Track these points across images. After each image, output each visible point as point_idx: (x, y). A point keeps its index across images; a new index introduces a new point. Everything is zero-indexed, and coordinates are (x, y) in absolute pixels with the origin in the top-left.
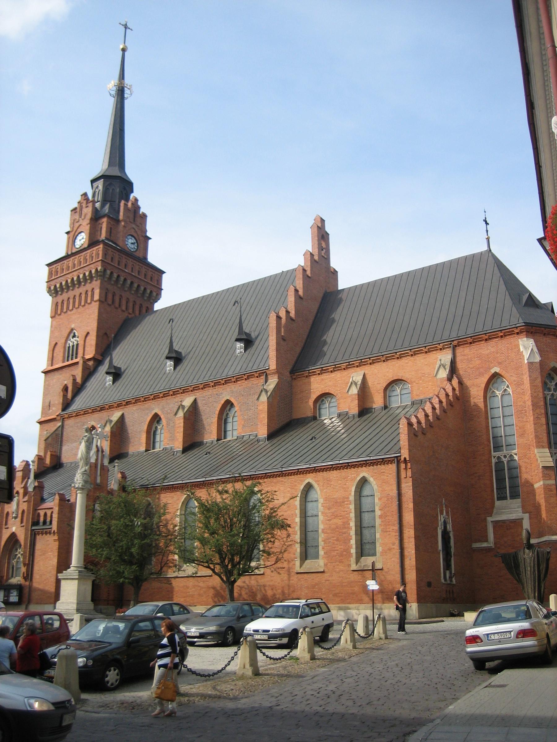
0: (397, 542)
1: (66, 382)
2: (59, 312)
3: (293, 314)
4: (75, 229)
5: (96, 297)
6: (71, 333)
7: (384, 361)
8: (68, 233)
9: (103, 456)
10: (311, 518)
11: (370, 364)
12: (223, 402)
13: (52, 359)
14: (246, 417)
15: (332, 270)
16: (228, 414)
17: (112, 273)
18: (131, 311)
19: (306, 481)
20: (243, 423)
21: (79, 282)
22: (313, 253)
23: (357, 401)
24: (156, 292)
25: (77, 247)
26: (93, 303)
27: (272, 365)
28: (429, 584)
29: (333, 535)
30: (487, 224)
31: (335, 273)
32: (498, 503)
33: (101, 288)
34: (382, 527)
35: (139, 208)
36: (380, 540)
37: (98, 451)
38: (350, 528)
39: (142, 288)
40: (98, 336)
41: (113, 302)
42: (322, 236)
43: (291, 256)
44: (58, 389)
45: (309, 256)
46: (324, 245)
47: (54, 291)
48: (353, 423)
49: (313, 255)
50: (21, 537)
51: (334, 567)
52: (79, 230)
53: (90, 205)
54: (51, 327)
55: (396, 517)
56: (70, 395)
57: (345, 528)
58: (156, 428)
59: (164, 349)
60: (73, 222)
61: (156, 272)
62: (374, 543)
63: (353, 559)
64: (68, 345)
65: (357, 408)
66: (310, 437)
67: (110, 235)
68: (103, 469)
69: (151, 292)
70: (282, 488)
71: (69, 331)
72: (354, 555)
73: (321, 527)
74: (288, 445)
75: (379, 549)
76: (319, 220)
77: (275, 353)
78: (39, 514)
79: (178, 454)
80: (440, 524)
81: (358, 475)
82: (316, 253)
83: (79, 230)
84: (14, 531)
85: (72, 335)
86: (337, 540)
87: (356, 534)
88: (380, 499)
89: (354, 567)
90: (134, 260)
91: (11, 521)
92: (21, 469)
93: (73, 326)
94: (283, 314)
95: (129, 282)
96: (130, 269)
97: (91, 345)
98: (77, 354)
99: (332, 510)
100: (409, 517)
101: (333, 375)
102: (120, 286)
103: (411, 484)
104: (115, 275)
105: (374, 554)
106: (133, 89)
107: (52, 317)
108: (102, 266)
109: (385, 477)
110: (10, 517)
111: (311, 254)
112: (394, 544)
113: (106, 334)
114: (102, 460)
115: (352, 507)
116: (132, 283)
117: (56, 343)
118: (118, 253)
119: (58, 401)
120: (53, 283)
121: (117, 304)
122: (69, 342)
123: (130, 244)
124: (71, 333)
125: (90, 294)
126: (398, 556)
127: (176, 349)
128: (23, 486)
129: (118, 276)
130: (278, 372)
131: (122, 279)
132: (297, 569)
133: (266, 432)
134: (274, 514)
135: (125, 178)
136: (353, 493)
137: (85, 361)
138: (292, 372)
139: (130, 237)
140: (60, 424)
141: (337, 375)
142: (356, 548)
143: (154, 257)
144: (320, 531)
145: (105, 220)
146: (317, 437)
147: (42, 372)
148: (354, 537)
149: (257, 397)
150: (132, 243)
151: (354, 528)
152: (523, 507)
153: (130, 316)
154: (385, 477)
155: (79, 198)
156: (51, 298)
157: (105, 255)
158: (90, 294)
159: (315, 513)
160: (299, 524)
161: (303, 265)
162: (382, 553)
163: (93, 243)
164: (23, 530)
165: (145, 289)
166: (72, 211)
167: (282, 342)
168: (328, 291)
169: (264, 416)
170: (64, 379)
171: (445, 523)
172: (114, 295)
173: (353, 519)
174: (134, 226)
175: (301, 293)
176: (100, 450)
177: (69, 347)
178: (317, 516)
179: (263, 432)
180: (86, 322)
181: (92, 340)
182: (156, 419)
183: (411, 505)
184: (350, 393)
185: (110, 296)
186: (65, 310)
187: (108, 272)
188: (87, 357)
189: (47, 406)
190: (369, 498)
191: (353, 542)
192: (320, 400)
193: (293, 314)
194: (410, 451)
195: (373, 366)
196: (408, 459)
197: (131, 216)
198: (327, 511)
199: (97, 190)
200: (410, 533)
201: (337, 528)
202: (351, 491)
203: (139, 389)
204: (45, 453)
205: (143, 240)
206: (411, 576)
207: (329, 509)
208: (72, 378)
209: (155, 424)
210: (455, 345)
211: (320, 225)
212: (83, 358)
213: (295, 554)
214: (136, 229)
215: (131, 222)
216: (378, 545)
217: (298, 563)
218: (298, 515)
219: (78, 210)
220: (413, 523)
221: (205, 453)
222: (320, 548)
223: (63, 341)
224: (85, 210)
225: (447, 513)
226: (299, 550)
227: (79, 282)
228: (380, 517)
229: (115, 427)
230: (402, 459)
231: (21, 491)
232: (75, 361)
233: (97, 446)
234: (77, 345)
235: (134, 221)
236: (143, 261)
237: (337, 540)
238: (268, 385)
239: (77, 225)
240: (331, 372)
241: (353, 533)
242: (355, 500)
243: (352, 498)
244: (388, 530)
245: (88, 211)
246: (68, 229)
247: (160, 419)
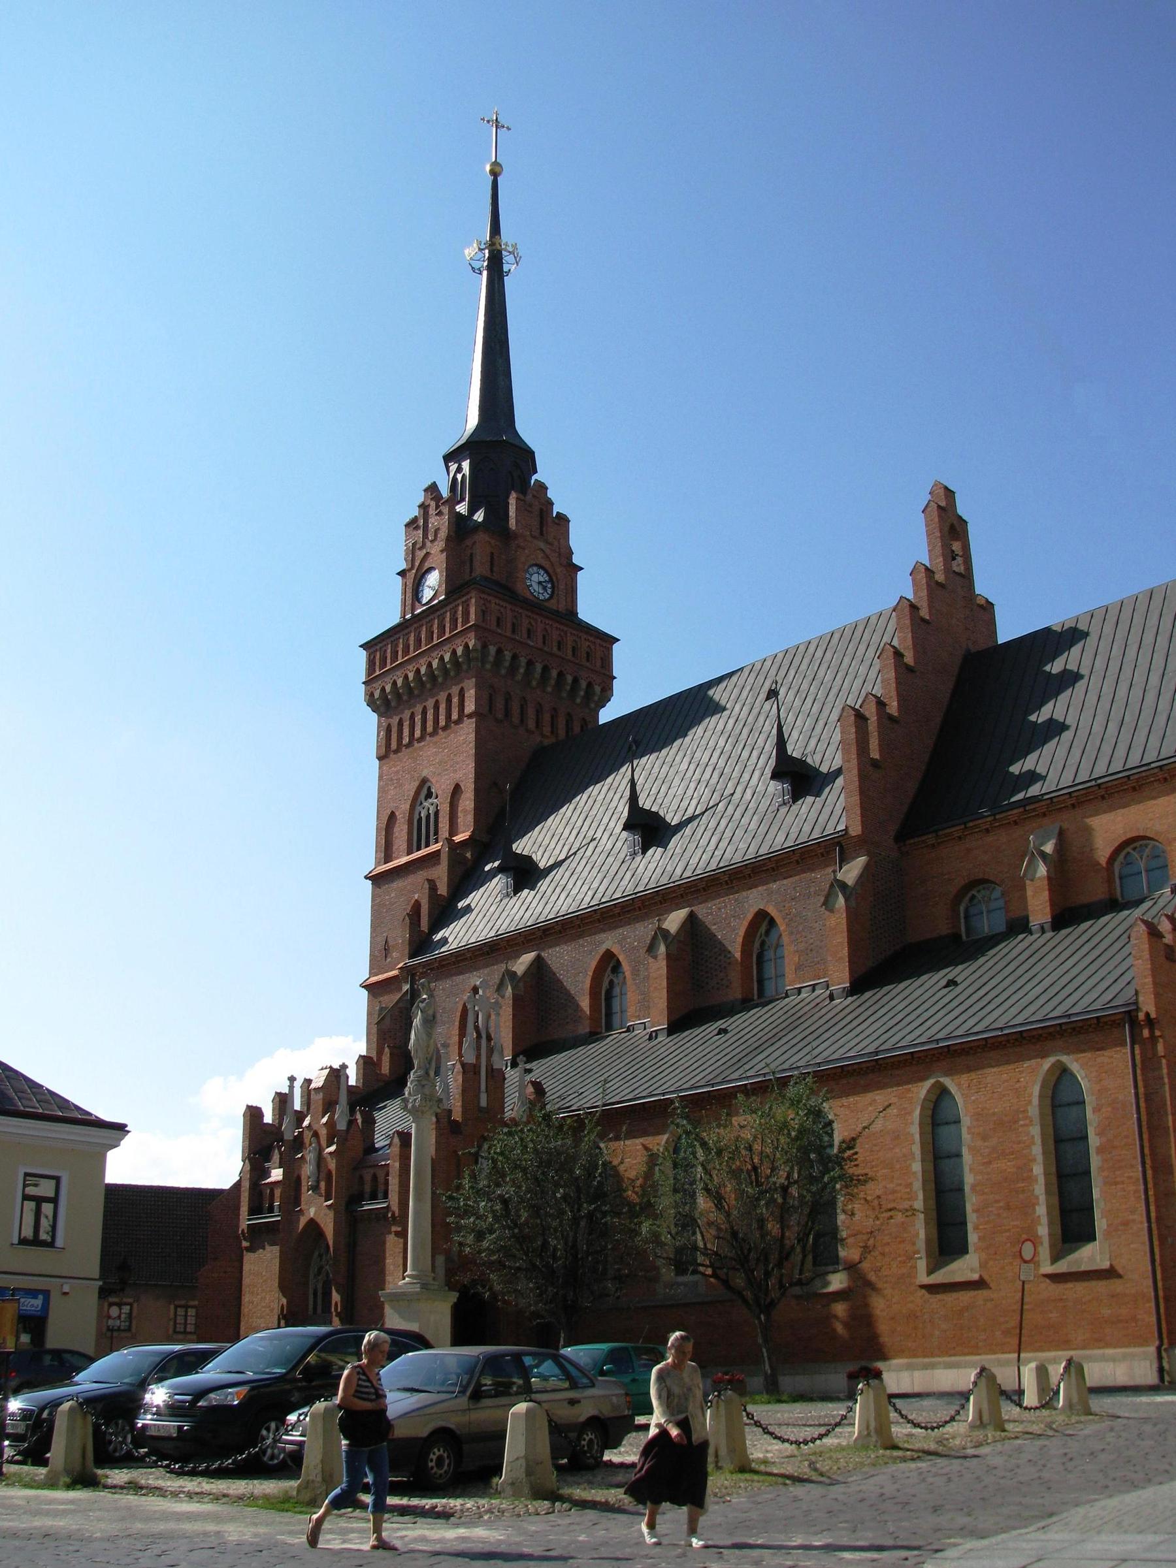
1: (416, 897)
2: (394, 746)
3: (893, 708)
4: (417, 564)
5: (470, 707)
6: (424, 790)
7: (1103, 797)
8: (402, 574)
9: (491, 1051)
10: (947, 1161)
11: (1073, 806)
12: (750, 916)
13: (386, 850)
14: (802, 946)
15: (983, 602)
16: (763, 943)
17: (499, 651)
18: (547, 730)
20: (796, 959)
22: (934, 569)
23: (1046, 893)
24: (601, 684)
25: (424, 601)
26: (467, 721)
29: (997, 1197)
31: (988, 607)
33: (478, 687)
34: (1105, 1173)
35: (550, 503)
36: (1102, 1205)
37: (479, 1036)
38: (1031, 1179)
39: (569, 679)
40: (477, 791)
41: (507, 713)
43: (881, 576)
44: (402, 908)
45: (922, 575)
46: (956, 546)
47: (381, 703)
48: (1042, 941)
49: (933, 573)
50: (328, 1227)
51: (1002, 1268)
52: (427, 565)
53: (445, 510)
54: (381, 778)
56: (424, 925)
58: (611, 983)
59: (620, 808)
60: (412, 551)
61: (598, 641)
64: (416, 817)
65: (1048, 909)
66: (943, 982)
67: (492, 570)
68: (493, 1077)
69: (590, 685)
71: (417, 784)
73: (969, 1179)
74: (893, 1003)
75: (1100, 1224)
76: (942, 491)
77: (858, 798)
78: (361, 1177)
79: (659, 1039)
82: (939, 566)
83: (427, 565)
84: (312, 1215)
85: (424, 792)
86: (1008, 1207)
87: (1048, 1192)
88: (1095, 1110)
90: (547, 618)
91: (307, 1194)
92: (320, 1084)
93: (425, 773)
95: (539, 668)
96: (540, 640)
97: (465, 811)
98: (436, 833)
101: (990, 839)
102: (519, 677)
104: (508, 655)
106: (521, 251)
107: (380, 758)
108: (478, 638)
110: (304, 1189)
111: (927, 569)
112: (1133, 1212)
113: (495, 784)
114: (489, 1057)
115: (1036, 1131)
116: (546, 669)
117: (393, 813)
118: (509, 606)
119: (400, 936)
120: (377, 685)
121: (516, 720)
122: (418, 808)
123: (535, 586)
124: (424, 790)
125: (455, 700)
127: (647, 807)
128: (325, 1120)
129: (515, 657)
131: (523, 661)
132: (923, 1278)
133: (846, 974)
134: (849, 1153)
135: (516, 442)
136: (1035, 1101)
137: (453, 847)
138: (901, 837)
139: (535, 569)
140: (406, 987)
142: (1050, 1224)
143: (592, 607)
144: (967, 1188)
146: (959, 979)
147: (366, 877)
148: (1042, 1199)
149: (822, 899)
150: (540, 583)
153: (546, 742)
154: (1106, 1060)
155: (420, 498)
156: (375, 716)
157: (483, 613)
158: (455, 700)
160: (920, 1175)
161: (910, 596)
162: (1108, 1234)
163: (455, 588)
164: (331, 1214)
165: (576, 680)
166: (407, 525)
168: (973, 650)
169: (838, 943)
170: (414, 889)
172: (508, 700)
173: (1040, 1158)
174: (542, 545)
175: (909, 659)
176: (484, 1036)
177: (420, 819)
178: (959, 1155)
179: (840, 977)
180: (452, 761)
181: (467, 802)
182: (609, 963)
185: (499, 704)
186: (406, 740)
187: (492, 650)
188: (458, 839)
189: (380, 953)
191: (1041, 1210)
192: (967, 898)
193: (893, 708)
194: (1157, 995)
196: (1153, 1015)
198: (979, 1143)
199: (459, 477)
202: (1031, 1095)
203: (569, 900)
204: (380, 1052)
205: (565, 572)
207: (985, 1138)
208: (426, 886)
209: (608, 976)
211: (943, 504)
212: (449, 840)
213: (914, 1244)
214: (548, 551)
215: (535, 537)
217: (922, 1265)
219: (421, 522)
221: (716, 1032)
222: (970, 1227)
223: (406, 806)
224: (433, 521)
226: (922, 1234)
228: (1100, 1150)
229: (521, 984)
230: (1141, 1016)
231: (323, 1132)
232: (434, 848)
233: (477, 1028)
234: (437, 813)
235: (542, 533)
237: (1008, 1207)
238: (847, 871)
239: (420, 554)
240: (987, 831)
241: (1039, 1189)
242: (1042, 1115)
243: (1034, 1110)
244: (1118, 1179)
245: (440, 523)
246: (403, 566)
247: (618, 963)
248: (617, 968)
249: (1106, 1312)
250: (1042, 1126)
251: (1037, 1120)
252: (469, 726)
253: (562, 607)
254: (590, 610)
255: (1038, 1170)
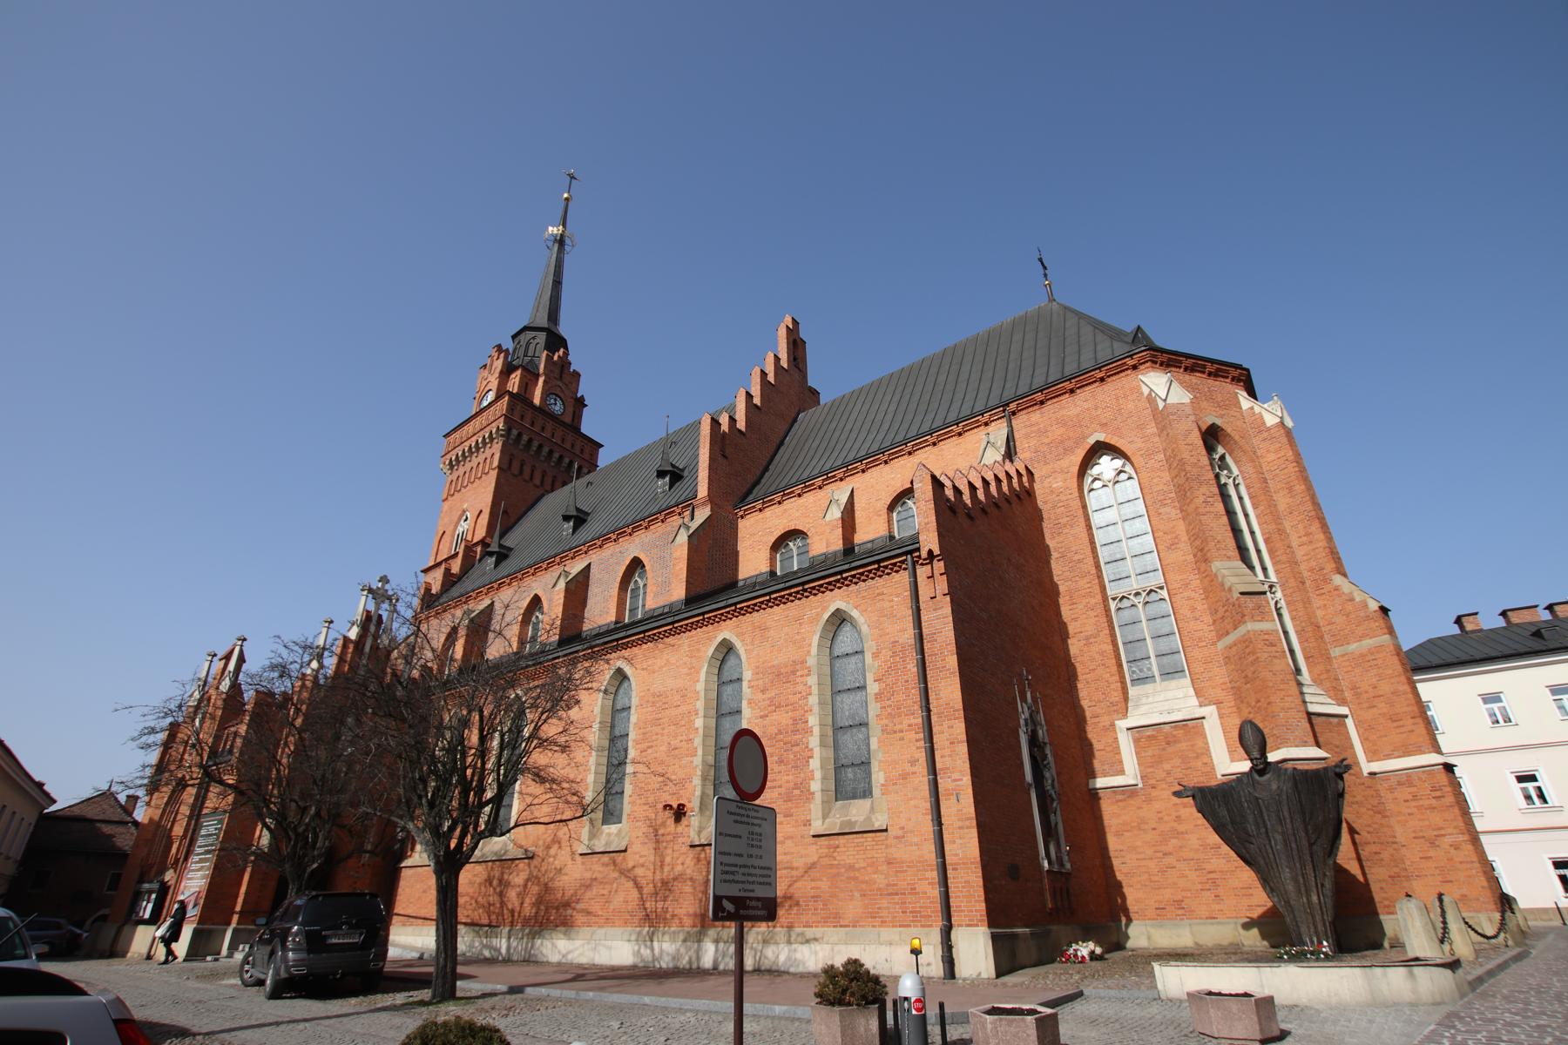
0: (922, 756)
3: (741, 425)
5: (496, 463)
19: (719, 639)
21: (478, 449)
27: (703, 491)
28: (1014, 872)
30: (1041, 260)
32: (1133, 691)
33: (502, 452)
34: (885, 721)
38: (809, 731)
41: (521, 472)
42: (796, 345)
55: (915, 694)
57: (795, 732)
62: (866, 764)
63: (816, 807)
70: (673, 660)
72: (818, 797)
75: (878, 777)
80: (1022, 722)
81: (824, 609)
87: (823, 745)
88: (876, 655)
89: (818, 826)
94: (724, 420)
99: (768, 695)
100: (948, 691)
103: (948, 610)
105: (867, 793)
109: (887, 605)
112: (913, 762)
115: (812, 680)
121: (526, 475)
126: (925, 790)
130: (711, 498)
136: (814, 650)
141: (809, 498)
142: (824, 778)
145: (519, 372)
148: (817, 752)
151: (816, 731)
152: (1198, 693)
159: (734, 705)
160: (701, 731)
163: (498, 398)
167: (721, 459)
171: (1032, 720)
173: (816, 709)
175: (757, 401)
178: (739, 712)
183: (953, 661)
184: (828, 517)
190: (853, 659)
191: (815, 763)
195: (867, 474)
197: (557, 371)
198: (760, 696)
200: (952, 733)
201: (780, 732)
206: (965, 845)
210: (1007, 408)
216: (875, 766)
218: (701, 713)
220: (960, 706)
225: (1034, 699)
227: (478, 449)
228: (878, 697)
236: (575, 427)
241: (814, 741)
242: (819, 665)
243: (811, 661)
244: (898, 727)
248: (541, 609)
249: (880, 880)
250: (819, 676)
251: (814, 670)
252: (494, 474)
253: (568, 419)
254: (588, 427)
255: (813, 720)
